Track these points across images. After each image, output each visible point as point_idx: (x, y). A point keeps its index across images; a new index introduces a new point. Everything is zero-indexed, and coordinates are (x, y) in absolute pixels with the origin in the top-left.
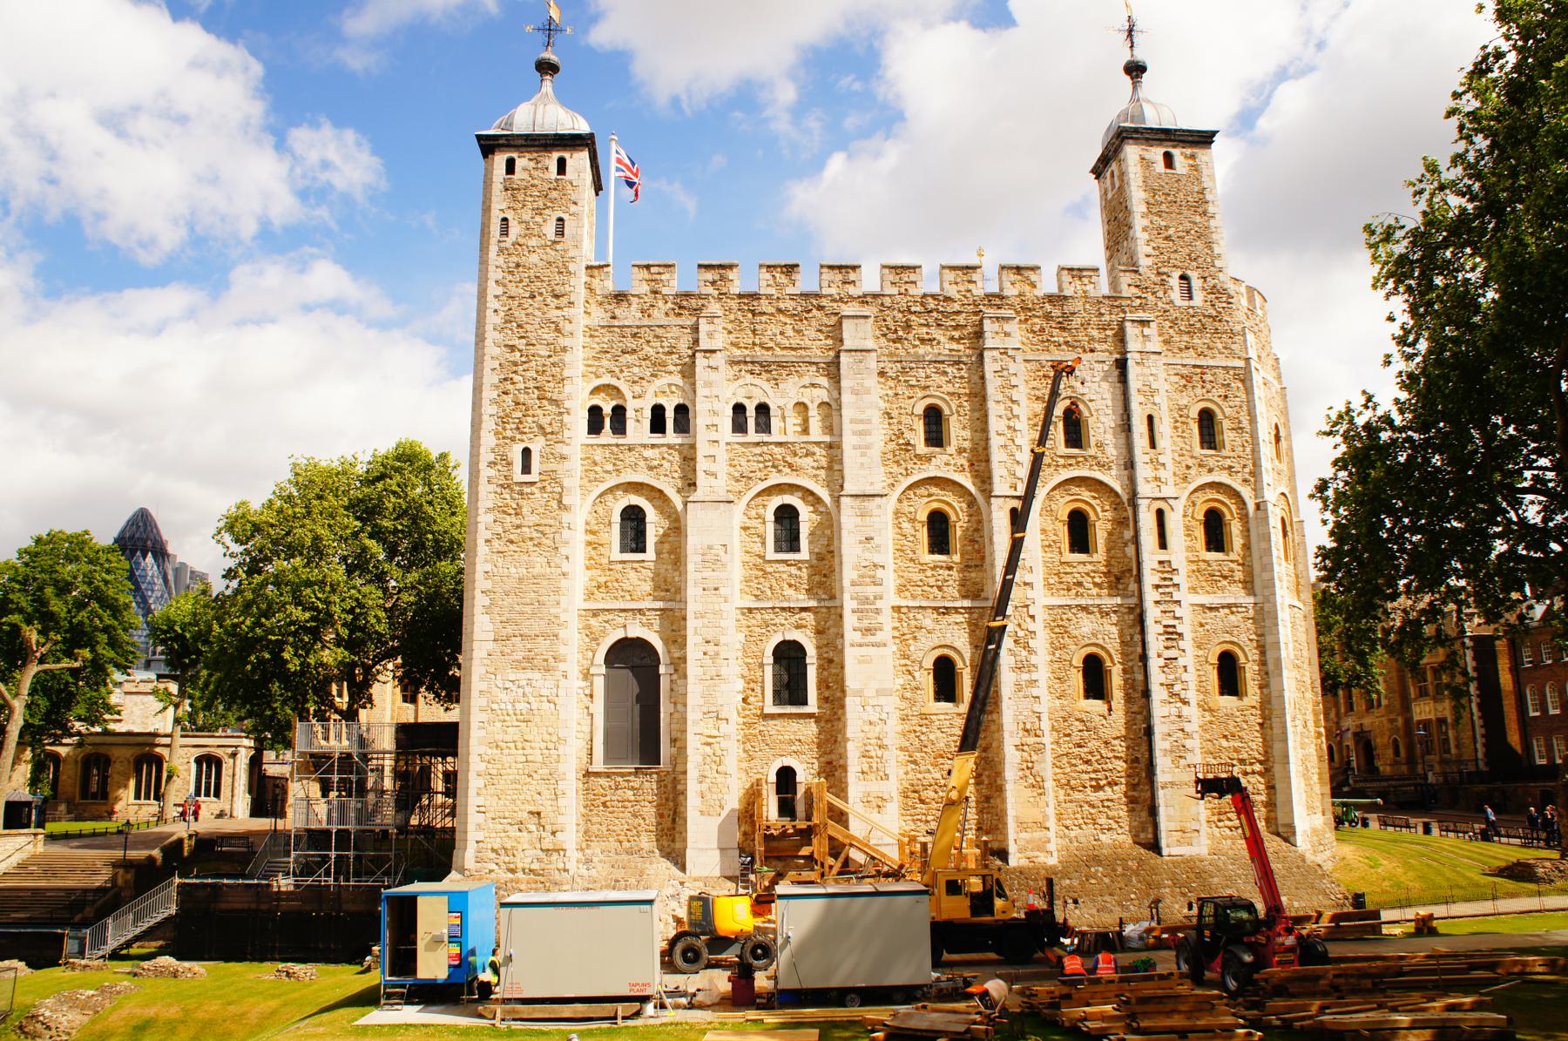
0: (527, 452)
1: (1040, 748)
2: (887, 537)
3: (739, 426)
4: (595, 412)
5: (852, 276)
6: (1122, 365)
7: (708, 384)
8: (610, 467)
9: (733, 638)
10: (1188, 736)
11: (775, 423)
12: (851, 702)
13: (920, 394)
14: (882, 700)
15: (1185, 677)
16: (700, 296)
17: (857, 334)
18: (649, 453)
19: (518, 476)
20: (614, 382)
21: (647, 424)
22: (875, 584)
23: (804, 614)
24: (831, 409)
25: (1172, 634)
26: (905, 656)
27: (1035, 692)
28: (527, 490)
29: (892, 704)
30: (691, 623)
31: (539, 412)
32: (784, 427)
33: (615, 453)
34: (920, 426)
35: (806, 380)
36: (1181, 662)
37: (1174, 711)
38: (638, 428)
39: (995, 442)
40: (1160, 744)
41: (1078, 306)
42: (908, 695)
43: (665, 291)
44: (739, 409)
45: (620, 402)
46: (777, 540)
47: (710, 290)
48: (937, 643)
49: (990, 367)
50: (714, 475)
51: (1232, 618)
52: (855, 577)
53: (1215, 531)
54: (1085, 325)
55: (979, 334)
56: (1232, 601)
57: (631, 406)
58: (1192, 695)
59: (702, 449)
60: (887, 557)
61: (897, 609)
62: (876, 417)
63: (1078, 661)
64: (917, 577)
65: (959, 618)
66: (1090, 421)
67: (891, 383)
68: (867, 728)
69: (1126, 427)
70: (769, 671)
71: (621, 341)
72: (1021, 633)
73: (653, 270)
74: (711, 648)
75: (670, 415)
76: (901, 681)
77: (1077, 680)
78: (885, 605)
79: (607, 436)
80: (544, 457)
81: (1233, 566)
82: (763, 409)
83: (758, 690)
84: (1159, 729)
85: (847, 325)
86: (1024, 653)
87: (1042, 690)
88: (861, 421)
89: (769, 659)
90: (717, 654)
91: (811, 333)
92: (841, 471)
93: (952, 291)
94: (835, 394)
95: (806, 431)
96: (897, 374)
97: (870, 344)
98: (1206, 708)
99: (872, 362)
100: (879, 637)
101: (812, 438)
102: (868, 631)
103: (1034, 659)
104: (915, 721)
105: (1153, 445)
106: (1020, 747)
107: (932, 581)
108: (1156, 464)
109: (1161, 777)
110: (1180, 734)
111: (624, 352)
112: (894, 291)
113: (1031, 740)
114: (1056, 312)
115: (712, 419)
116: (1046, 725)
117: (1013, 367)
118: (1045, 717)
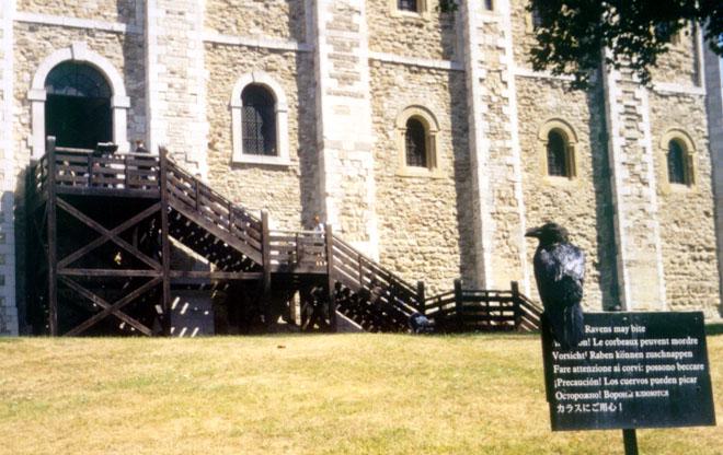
10: (648, 215)
12: (329, 156)
14: (361, 155)
15: (645, 158)
22: (350, 28)
23: (273, 57)
26: (380, 114)
27: (509, 160)
29: (369, 161)
30: (154, 51)
36: (641, 143)
37: (636, 191)
40: (624, 222)
42: (383, 154)
48: (410, 103)
51: (680, 106)
52: (331, 19)
56: (680, 90)
58: (650, 176)
61: (371, 61)
63: (544, 134)
64: (388, 31)
65: (431, 79)
68: (345, 184)
70: (237, 115)
72: (495, 99)
74: (176, 80)
76: (375, 139)
77: (542, 154)
78: (364, 53)
81: (680, 57)
83: (226, 135)
84: (622, 208)
86: (498, 119)
87: (516, 158)
89: (237, 101)
90: (184, 88)
98: (660, 194)
100: (357, 87)
102: (345, 79)
103: (507, 126)
106: (495, 215)
107: (403, 37)
110: (641, 214)
113: (506, 209)
116: (519, 195)
118: (518, 186)
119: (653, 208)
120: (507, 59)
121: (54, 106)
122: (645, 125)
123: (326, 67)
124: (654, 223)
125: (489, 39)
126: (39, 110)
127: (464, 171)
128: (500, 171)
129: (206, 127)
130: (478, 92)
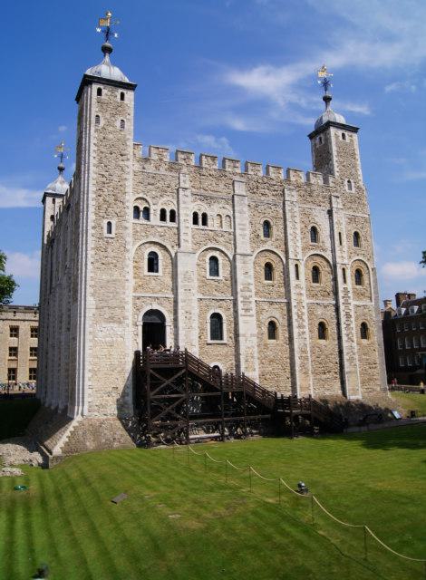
0: (109, 224)
1: (307, 358)
2: (252, 273)
3: (195, 222)
4: (136, 209)
5: (237, 165)
6: (330, 213)
7: (184, 203)
8: (144, 234)
9: (196, 311)
10: (354, 354)
11: (209, 222)
12: (241, 339)
16: (179, 165)
17: (240, 189)
18: (159, 229)
19: (106, 234)
20: (145, 197)
24: (232, 218)
25: (348, 316)
27: (305, 336)
28: (110, 241)
29: (255, 340)
31: (115, 206)
32: (213, 223)
33: (146, 229)
34: (262, 229)
38: (155, 218)
39: (290, 237)
40: (346, 357)
41: (315, 188)
43: (165, 160)
44: (195, 215)
46: (210, 270)
47: (183, 162)
49: (287, 208)
50: (187, 241)
53: (359, 276)
54: (318, 196)
55: (283, 195)
58: (355, 339)
59: (182, 231)
60: (252, 281)
63: (317, 324)
66: (320, 232)
67: (253, 210)
69: (332, 237)
71: (147, 180)
74: (188, 316)
75: (168, 214)
78: (253, 299)
79: (142, 220)
80: (117, 228)
82: (205, 216)
84: (345, 351)
85: (236, 184)
88: (243, 225)
91: (222, 186)
92: (235, 244)
93: (272, 176)
95: (221, 226)
97: (244, 194)
99: (246, 201)
101: (224, 229)
102: (247, 310)
104: (263, 347)
105: (341, 244)
108: (341, 250)
109: (346, 370)
111: (149, 184)
114: (309, 189)
117: (296, 209)
119: (356, 351)
120: (304, 298)
121: (145, 325)
122: (353, 319)
123: (240, 306)
124: (356, 357)
125: (298, 291)
126: (140, 328)
127: (291, 339)
128: (302, 341)
129: (198, 331)
130: (294, 311)
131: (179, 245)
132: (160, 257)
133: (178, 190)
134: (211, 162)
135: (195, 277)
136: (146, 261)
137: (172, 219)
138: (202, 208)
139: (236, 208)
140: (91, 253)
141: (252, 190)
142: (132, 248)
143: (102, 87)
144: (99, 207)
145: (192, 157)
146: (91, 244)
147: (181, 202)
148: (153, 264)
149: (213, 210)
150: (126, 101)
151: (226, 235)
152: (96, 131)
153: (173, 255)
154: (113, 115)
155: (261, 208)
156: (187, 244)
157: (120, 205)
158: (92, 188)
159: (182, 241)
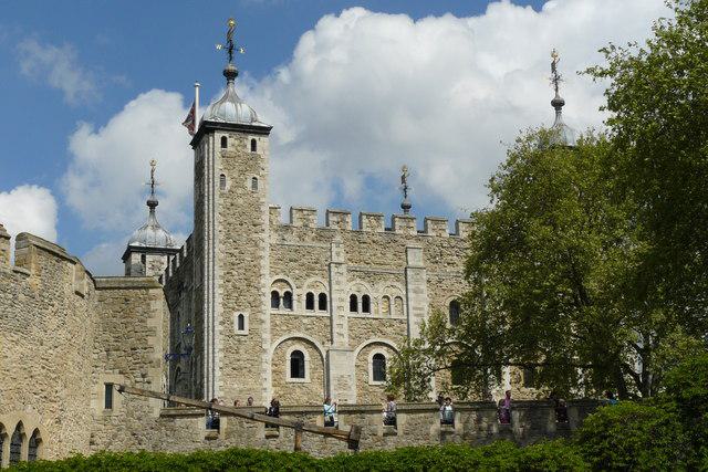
0: (241, 317)
3: (354, 308)
4: (275, 295)
5: (412, 224)
7: (338, 283)
8: (285, 328)
13: (449, 294)
17: (416, 258)
18: (305, 321)
21: (304, 303)
32: (378, 309)
35: (389, 283)
38: (299, 307)
43: (311, 225)
44: (353, 299)
45: (289, 290)
47: (336, 227)
50: (342, 335)
57: (295, 293)
62: (425, 306)
71: (288, 257)
73: (305, 212)
75: (316, 299)
79: (283, 310)
82: (366, 299)
88: (420, 309)
91: (390, 256)
94: (404, 292)
96: (436, 284)
97: (421, 264)
112: (434, 234)
115: (340, 302)
131: (332, 340)
132: (307, 357)
133: (329, 266)
134: (374, 223)
135: (353, 383)
136: (288, 364)
137: (323, 306)
138: (365, 288)
139: (410, 286)
140: (219, 355)
141: (434, 259)
142: (270, 347)
143: (227, 135)
144: (228, 296)
145: (349, 219)
146: (219, 346)
147: (333, 282)
148: (297, 367)
149: (377, 291)
150: (259, 151)
151: (396, 324)
152: (222, 195)
153: (324, 355)
154: (242, 172)
155: (446, 284)
156: (342, 338)
157: (253, 291)
158: (219, 272)
159: (335, 335)
